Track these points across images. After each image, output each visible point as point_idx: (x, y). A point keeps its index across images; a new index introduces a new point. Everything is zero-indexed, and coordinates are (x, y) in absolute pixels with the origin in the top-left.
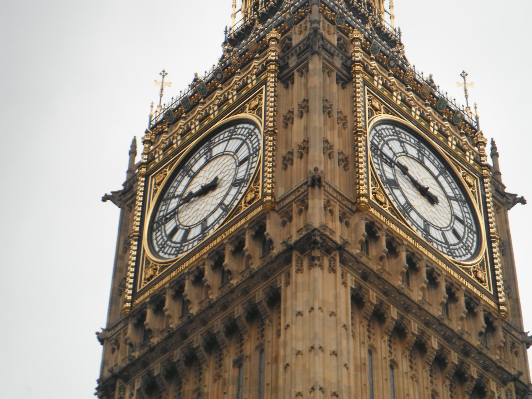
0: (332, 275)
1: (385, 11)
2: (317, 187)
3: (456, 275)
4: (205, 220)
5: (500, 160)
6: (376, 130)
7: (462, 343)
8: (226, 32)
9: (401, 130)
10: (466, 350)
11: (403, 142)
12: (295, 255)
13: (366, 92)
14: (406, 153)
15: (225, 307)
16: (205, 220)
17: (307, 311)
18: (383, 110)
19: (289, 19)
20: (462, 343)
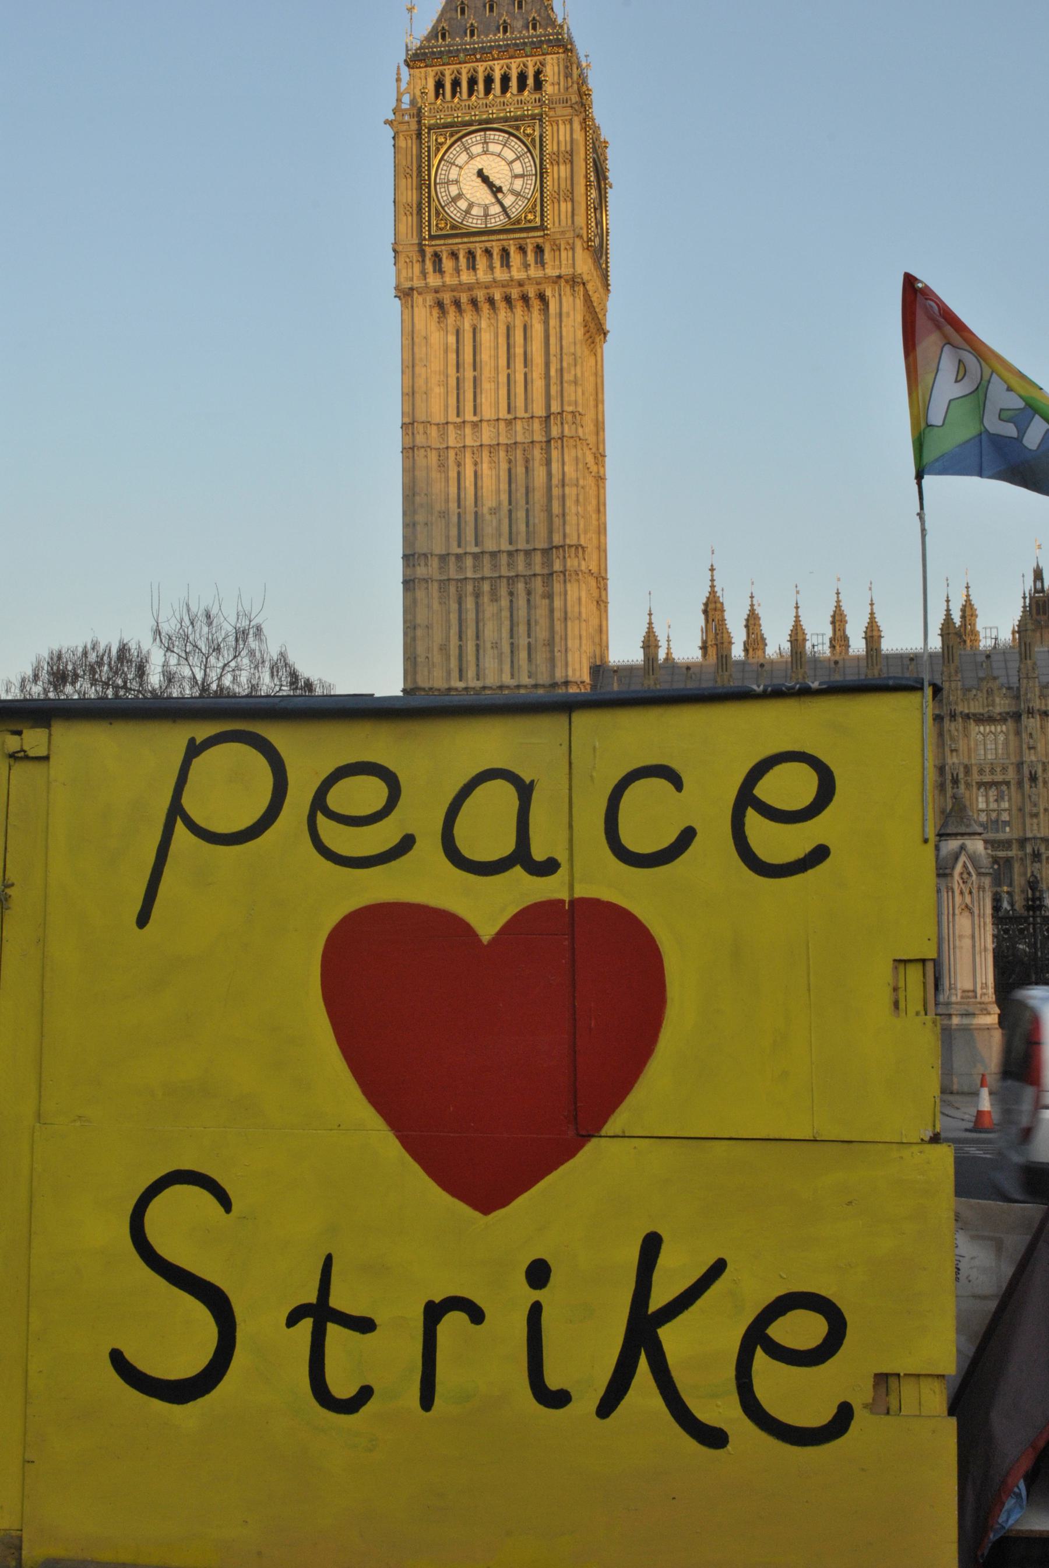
10: (521, 284)
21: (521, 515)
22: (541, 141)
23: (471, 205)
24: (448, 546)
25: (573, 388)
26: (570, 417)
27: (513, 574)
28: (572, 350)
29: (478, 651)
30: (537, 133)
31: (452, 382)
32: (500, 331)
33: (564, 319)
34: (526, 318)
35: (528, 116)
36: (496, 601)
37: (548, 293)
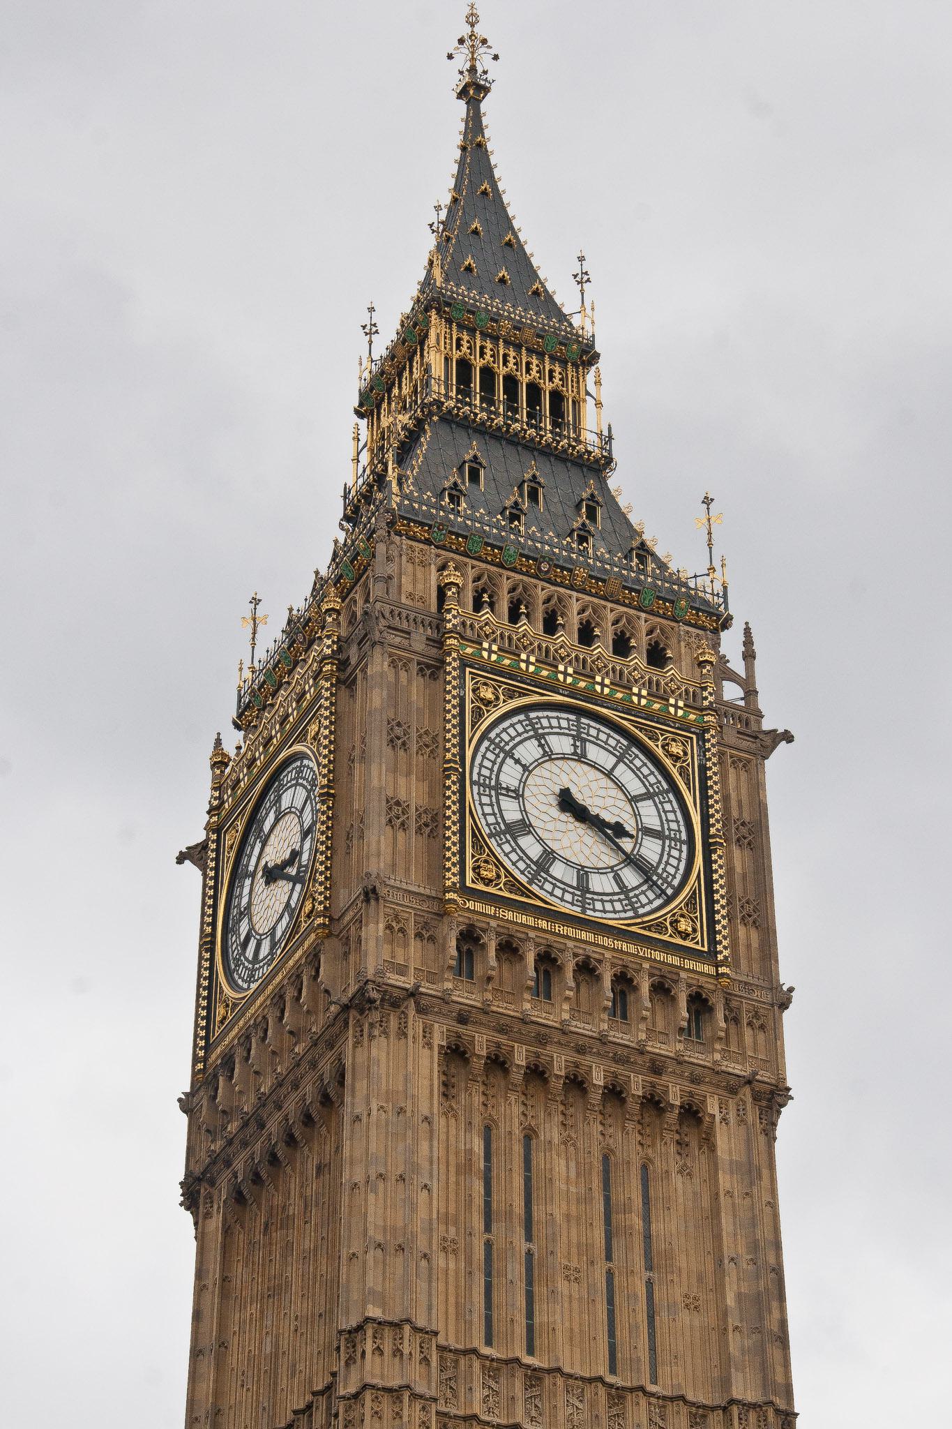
0: (403, 1041)
1: (588, 393)
2: (373, 902)
3: (632, 949)
4: (274, 928)
5: (757, 663)
6: (489, 739)
7: (648, 1057)
8: (345, 497)
9: (540, 714)
10: (656, 1068)
11: (543, 736)
12: (353, 1013)
13: (468, 677)
14: (549, 756)
15: (296, 1086)
16: (274, 928)
17: (365, 1114)
18: (502, 697)
19: (365, 549)
20: (648, 1057)
22: (704, 779)
25: (778, 1354)
35: (675, 719)
37: (712, 1106)
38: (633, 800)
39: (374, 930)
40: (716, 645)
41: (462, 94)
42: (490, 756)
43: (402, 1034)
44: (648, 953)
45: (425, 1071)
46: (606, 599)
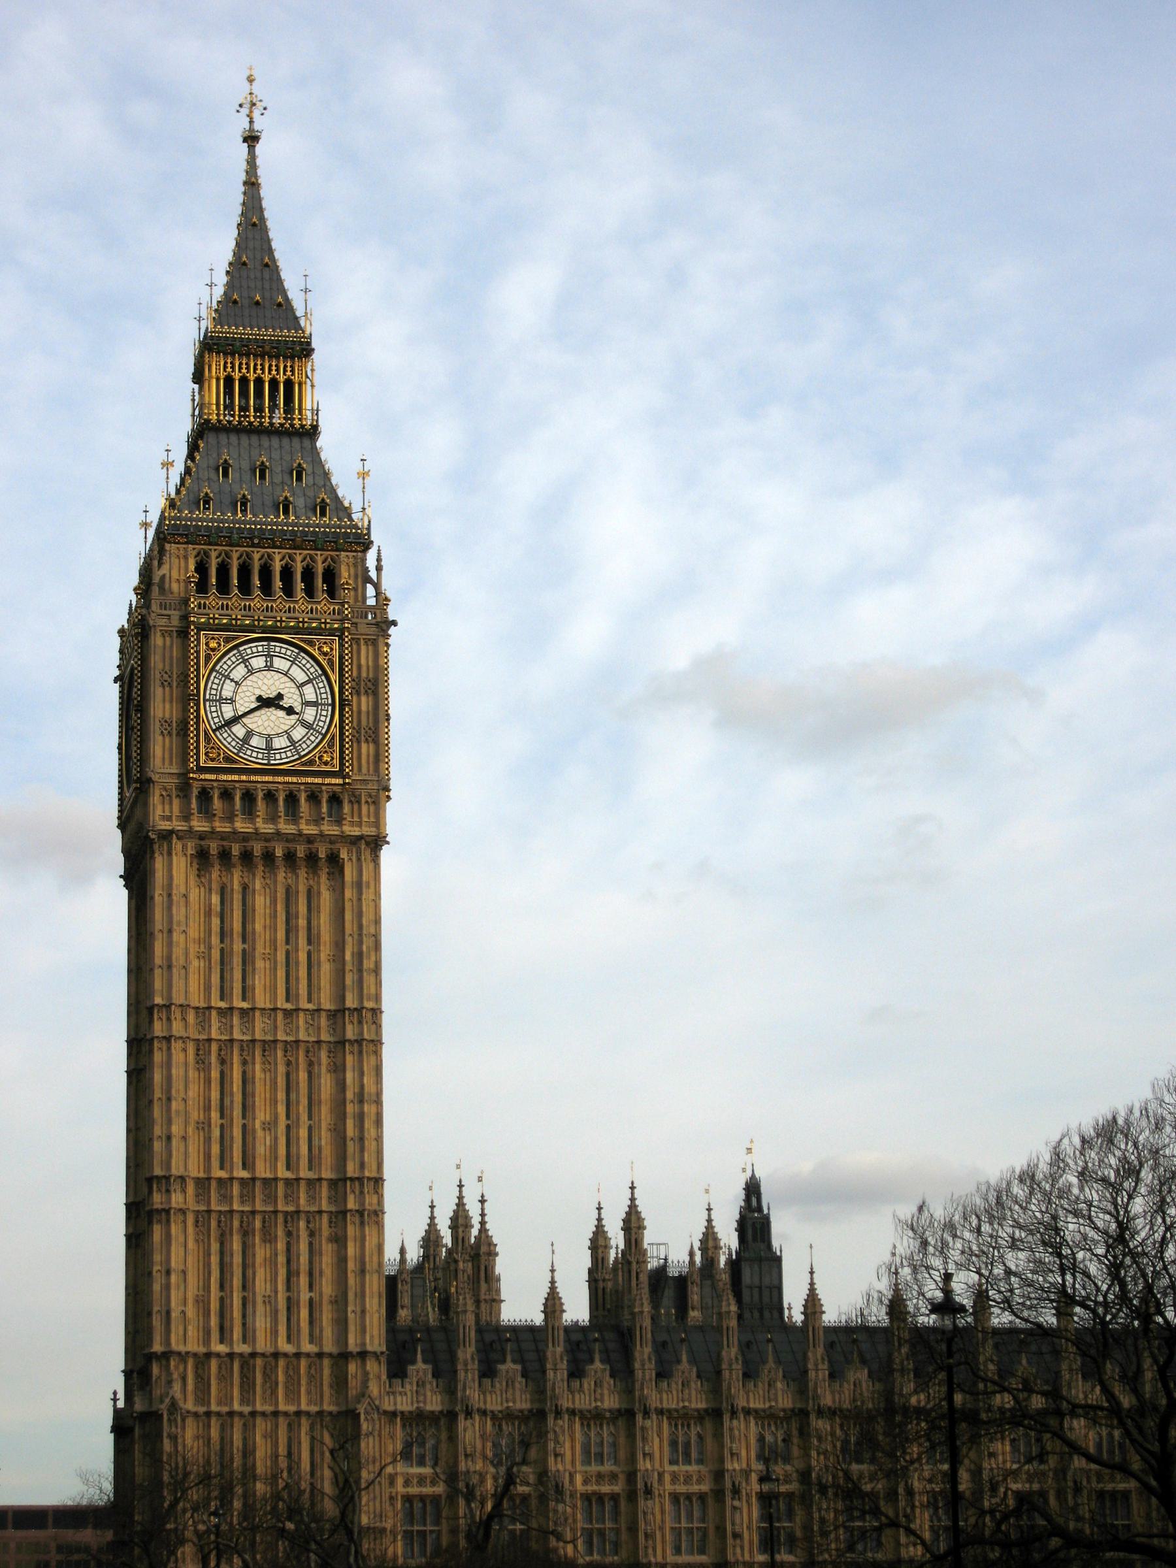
1: (307, 377)
3: (294, 780)
10: (310, 840)
14: (251, 672)
21: (303, 1133)
22: (341, 664)
23: (250, 734)
24: (208, 1168)
25: (373, 979)
26: (369, 1015)
27: (291, 1208)
28: (372, 931)
29: (244, 1305)
30: (336, 653)
31: (216, 955)
32: (279, 895)
33: (364, 890)
34: (311, 882)
36: (270, 1242)
37: (344, 855)
38: (300, 686)
39: (155, 798)
40: (364, 560)
41: (245, 140)
42: (217, 681)
43: (170, 854)
44: (303, 780)
45: (183, 870)
46: (295, 548)
